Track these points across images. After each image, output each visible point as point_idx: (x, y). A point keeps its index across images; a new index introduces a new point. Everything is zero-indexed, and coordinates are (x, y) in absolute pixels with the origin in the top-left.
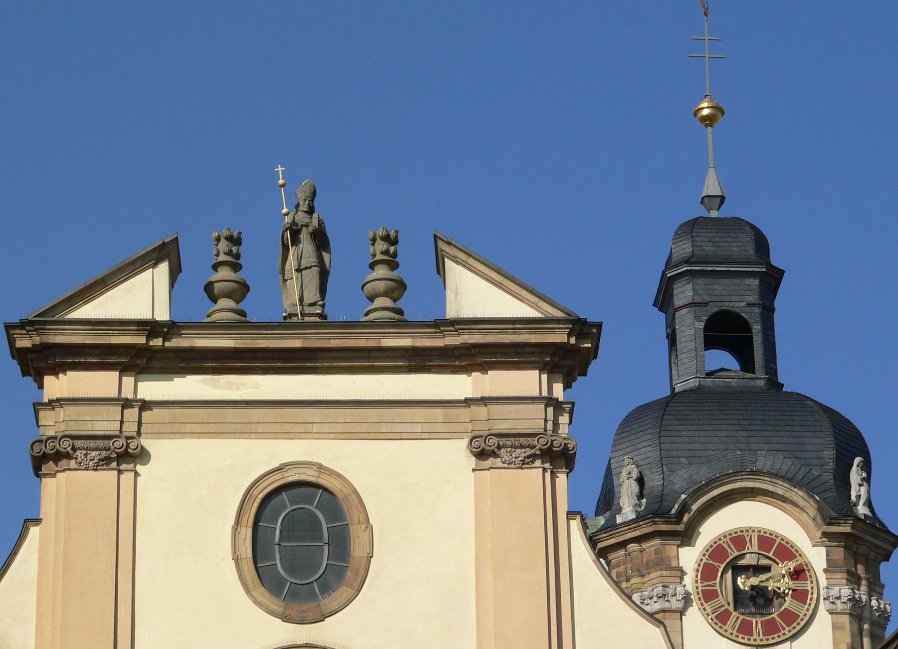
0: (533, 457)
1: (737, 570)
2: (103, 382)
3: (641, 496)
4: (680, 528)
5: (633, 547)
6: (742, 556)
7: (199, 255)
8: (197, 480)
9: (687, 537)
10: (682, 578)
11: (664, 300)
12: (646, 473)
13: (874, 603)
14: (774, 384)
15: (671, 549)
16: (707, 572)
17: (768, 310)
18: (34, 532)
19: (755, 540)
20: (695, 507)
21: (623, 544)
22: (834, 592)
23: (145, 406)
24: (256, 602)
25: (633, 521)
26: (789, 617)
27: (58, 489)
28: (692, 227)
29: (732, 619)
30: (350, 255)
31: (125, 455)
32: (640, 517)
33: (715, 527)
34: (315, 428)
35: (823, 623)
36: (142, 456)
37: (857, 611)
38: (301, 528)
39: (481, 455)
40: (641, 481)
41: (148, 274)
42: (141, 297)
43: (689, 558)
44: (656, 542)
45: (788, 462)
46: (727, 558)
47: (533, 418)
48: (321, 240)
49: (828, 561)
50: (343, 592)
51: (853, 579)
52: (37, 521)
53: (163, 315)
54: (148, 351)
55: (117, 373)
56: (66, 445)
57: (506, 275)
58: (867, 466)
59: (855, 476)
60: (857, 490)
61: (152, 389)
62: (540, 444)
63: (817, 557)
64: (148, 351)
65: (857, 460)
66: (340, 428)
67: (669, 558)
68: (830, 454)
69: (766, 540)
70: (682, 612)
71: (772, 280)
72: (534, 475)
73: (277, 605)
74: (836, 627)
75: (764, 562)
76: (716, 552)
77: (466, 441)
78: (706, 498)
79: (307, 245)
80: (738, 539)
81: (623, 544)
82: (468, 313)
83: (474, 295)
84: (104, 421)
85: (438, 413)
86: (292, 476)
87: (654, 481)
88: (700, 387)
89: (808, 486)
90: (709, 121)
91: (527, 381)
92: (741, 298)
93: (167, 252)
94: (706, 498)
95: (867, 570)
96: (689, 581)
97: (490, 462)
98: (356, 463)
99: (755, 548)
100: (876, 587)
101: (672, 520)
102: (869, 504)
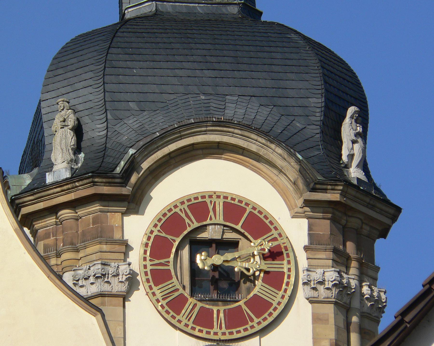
1: (197, 245)
3: (77, 149)
4: (126, 190)
5: (65, 213)
6: (203, 228)
9: (134, 203)
10: (126, 255)
12: (85, 120)
13: (365, 290)
15: (113, 218)
16: (158, 248)
19: (220, 209)
20: (145, 165)
21: (53, 210)
22: (317, 275)
25: (66, 181)
26: (260, 306)
29: (188, 307)
32: (76, 176)
35: (301, 313)
37: (344, 301)
40: (78, 130)
43: (137, 228)
44: (96, 207)
45: (265, 111)
46: (184, 230)
49: (311, 236)
51: (341, 260)
58: (362, 118)
59: (348, 130)
60: (350, 148)
63: (296, 231)
65: (351, 110)
67: (112, 229)
68: (316, 102)
69: (234, 209)
70: (125, 298)
74: (317, 319)
75: (230, 236)
76: (171, 222)
78: (159, 154)
80: (199, 206)
81: (53, 210)
87: (95, 131)
88: (157, 13)
89: (288, 141)
94: (159, 154)
95: (359, 249)
96: (135, 258)
99: (220, 219)
100: (368, 270)
101: (114, 180)
102: (364, 166)
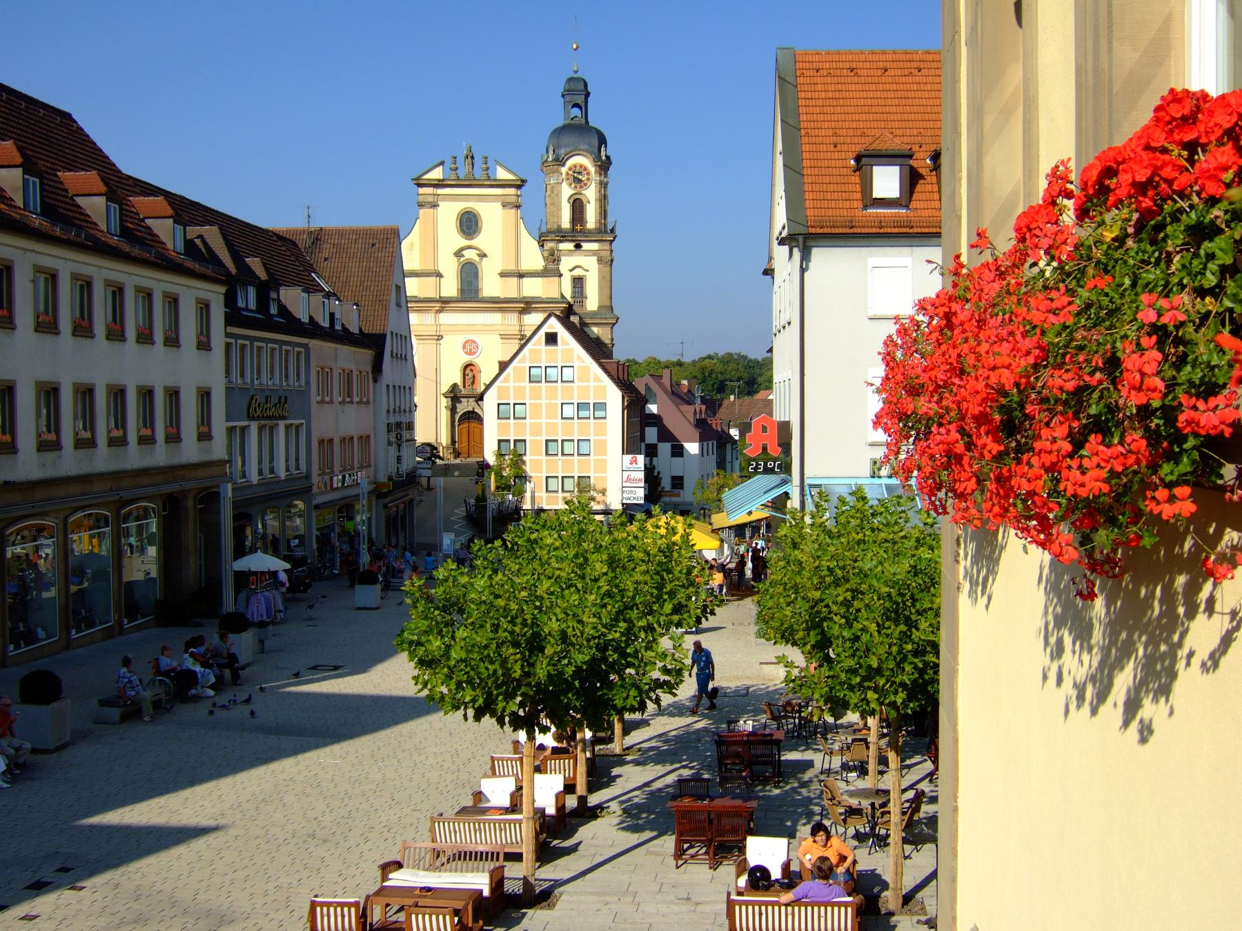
2: (430, 190)
8: (449, 211)
9: (563, 165)
14: (587, 122)
17: (586, 102)
27: (422, 212)
28: (570, 80)
30: (478, 161)
31: (435, 206)
33: (570, 163)
35: (593, 185)
37: (601, 183)
38: (469, 220)
42: (437, 174)
43: (564, 170)
47: (513, 199)
48: (473, 158)
54: (439, 184)
57: (509, 170)
60: (603, 153)
61: (440, 191)
63: (592, 169)
64: (439, 184)
71: (588, 95)
72: (513, 211)
83: (502, 174)
84: (431, 199)
89: (591, 153)
91: (512, 191)
92: (580, 99)
93: (442, 163)
98: (479, 207)
100: (606, 176)
101: (560, 161)
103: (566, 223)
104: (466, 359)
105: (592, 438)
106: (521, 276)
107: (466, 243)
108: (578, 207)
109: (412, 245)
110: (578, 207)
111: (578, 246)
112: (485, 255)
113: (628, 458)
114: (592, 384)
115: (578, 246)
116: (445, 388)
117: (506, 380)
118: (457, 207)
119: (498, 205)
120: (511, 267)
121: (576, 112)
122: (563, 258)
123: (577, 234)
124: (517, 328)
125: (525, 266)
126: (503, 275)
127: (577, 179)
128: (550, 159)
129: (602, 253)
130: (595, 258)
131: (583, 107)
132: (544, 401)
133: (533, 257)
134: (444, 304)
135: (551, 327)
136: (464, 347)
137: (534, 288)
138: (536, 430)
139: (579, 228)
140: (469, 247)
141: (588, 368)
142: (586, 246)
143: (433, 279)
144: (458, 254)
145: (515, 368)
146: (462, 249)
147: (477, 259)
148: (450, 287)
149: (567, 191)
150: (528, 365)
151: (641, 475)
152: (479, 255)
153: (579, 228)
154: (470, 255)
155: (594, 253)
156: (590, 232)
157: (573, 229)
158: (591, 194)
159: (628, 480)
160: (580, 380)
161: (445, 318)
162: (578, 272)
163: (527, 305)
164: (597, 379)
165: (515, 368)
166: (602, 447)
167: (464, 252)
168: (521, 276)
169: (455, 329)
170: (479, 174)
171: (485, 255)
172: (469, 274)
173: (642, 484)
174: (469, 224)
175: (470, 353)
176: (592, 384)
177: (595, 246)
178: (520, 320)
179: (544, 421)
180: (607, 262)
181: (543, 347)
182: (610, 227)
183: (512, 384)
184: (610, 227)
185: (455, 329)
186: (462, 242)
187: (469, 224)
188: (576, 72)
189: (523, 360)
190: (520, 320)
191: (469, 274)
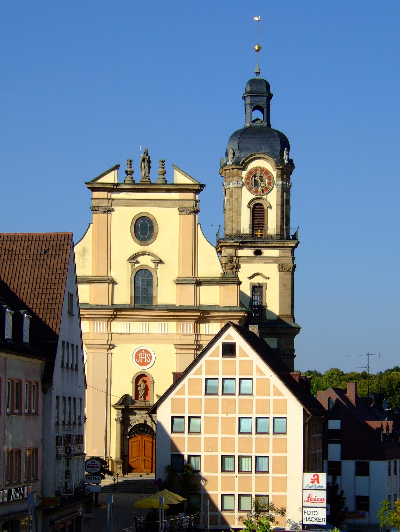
0: (191, 212)
2: (104, 194)
3: (234, 157)
4: (242, 167)
5: (231, 170)
6: (256, 174)
7: (124, 167)
8: (123, 217)
9: (244, 169)
10: (242, 179)
11: (244, 98)
12: (235, 152)
13: (287, 184)
14: (269, 125)
15: (240, 171)
16: (248, 178)
18: (91, 225)
19: (260, 170)
20: (246, 162)
21: (229, 170)
22: (277, 183)
23: (113, 199)
24: (135, 242)
25: (231, 165)
27: (96, 217)
28: (252, 82)
29: (253, 189)
30: (155, 165)
31: (109, 210)
32: (233, 164)
33: (251, 166)
34: (147, 205)
35: (275, 189)
36: (113, 210)
39: (181, 211)
40: (234, 154)
41: (113, 172)
43: (244, 174)
44: (236, 170)
45: (269, 150)
46: (253, 174)
47: (191, 204)
48: (149, 162)
49: (277, 175)
50: (152, 240)
51: (282, 179)
52: (92, 223)
53: (116, 182)
54: (115, 188)
55: (107, 192)
56: (97, 209)
57: (186, 174)
58: (288, 150)
59: (285, 153)
60: (285, 157)
61: (115, 195)
62: (192, 210)
63: (274, 174)
64: (115, 188)
65: (286, 149)
66: (152, 205)
67: (239, 174)
68: (279, 148)
69: (262, 170)
70: (242, 188)
71: (270, 96)
72: (191, 216)
73: (139, 242)
74: (277, 191)
75: (261, 175)
76: (250, 173)
77: (177, 208)
78: (249, 160)
79: (146, 163)
80: (256, 169)
81: (229, 170)
82: (178, 183)
83: (180, 179)
85: (172, 202)
86: (142, 215)
87: (237, 155)
88: (251, 127)
89: (272, 156)
90: (258, 51)
91: (190, 196)
92: (262, 102)
93: (117, 167)
94: (249, 160)
95: (286, 176)
96: (243, 180)
97: (182, 213)
99: (260, 172)
100: (288, 180)
103: (245, 227)
104: (138, 369)
105: (271, 454)
106: (198, 283)
107: (138, 248)
108: (258, 212)
109: (84, 250)
110: (258, 212)
111: (258, 253)
112: (161, 262)
113: (309, 476)
114: (272, 397)
115: (258, 253)
116: (115, 400)
117: (181, 392)
118: (134, 211)
119: (175, 210)
120: (188, 274)
121: (258, 114)
122: (242, 265)
123: (256, 240)
124: (193, 337)
125: (202, 273)
126: (179, 282)
127: (257, 181)
128: (230, 163)
129: (284, 260)
130: (276, 265)
131: (265, 109)
132: (220, 415)
133: (210, 263)
134: (115, 312)
135: (229, 337)
136: (137, 357)
137: (210, 296)
138: (212, 445)
139: (259, 233)
140: (144, 254)
141: (268, 381)
142: (267, 253)
143: (105, 286)
144: (133, 259)
145: (190, 379)
146: (136, 255)
147: (152, 265)
148: (123, 295)
149: (247, 196)
150: (204, 376)
151: (323, 495)
152: (154, 262)
153: (259, 233)
154: (145, 261)
155: (274, 260)
156: (271, 238)
157: (253, 235)
158: (272, 198)
159: (310, 499)
160: (258, 394)
161: (117, 327)
162: (257, 280)
163: (204, 315)
164: (277, 392)
165: (190, 379)
166: (281, 464)
167: (140, 259)
168: (198, 283)
169: (128, 338)
170: (155, 177)
171: (161, 262)
172: (143, 282)
173: (325, 504)
174: (144, 229)
175: (143, 364)
176: (272, 397)
177: (275, 253)
178: (196, 329)
179: (220, 436)
180: (289, 270)
181: (220, 358)
182: (292, 233)
183: (186, 397)
184: (292, 233)
185: (128, 338)
186: (137, 248)
187: (144, 229)
188: (258, 73)
189: (199, 372)
190: (196, 329)
191: (143, 282)
